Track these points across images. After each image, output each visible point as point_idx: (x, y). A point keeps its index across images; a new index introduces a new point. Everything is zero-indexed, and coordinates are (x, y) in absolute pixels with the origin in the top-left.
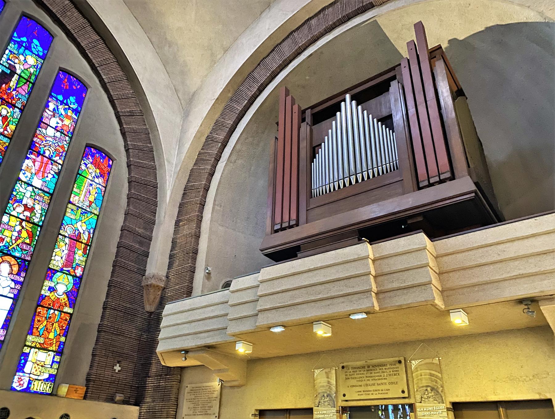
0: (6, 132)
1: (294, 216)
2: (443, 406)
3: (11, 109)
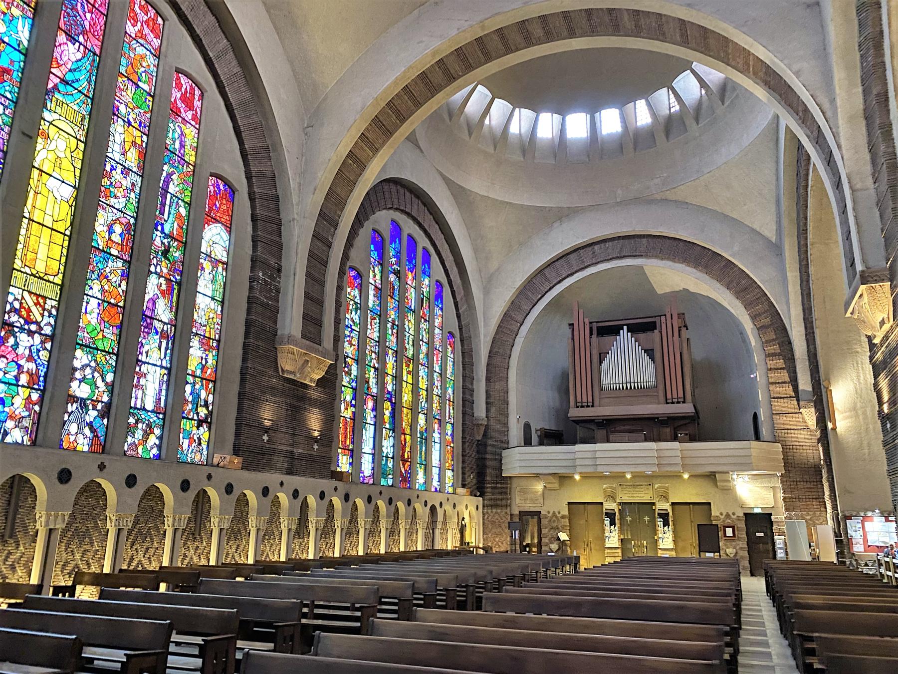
1: (590, 399)
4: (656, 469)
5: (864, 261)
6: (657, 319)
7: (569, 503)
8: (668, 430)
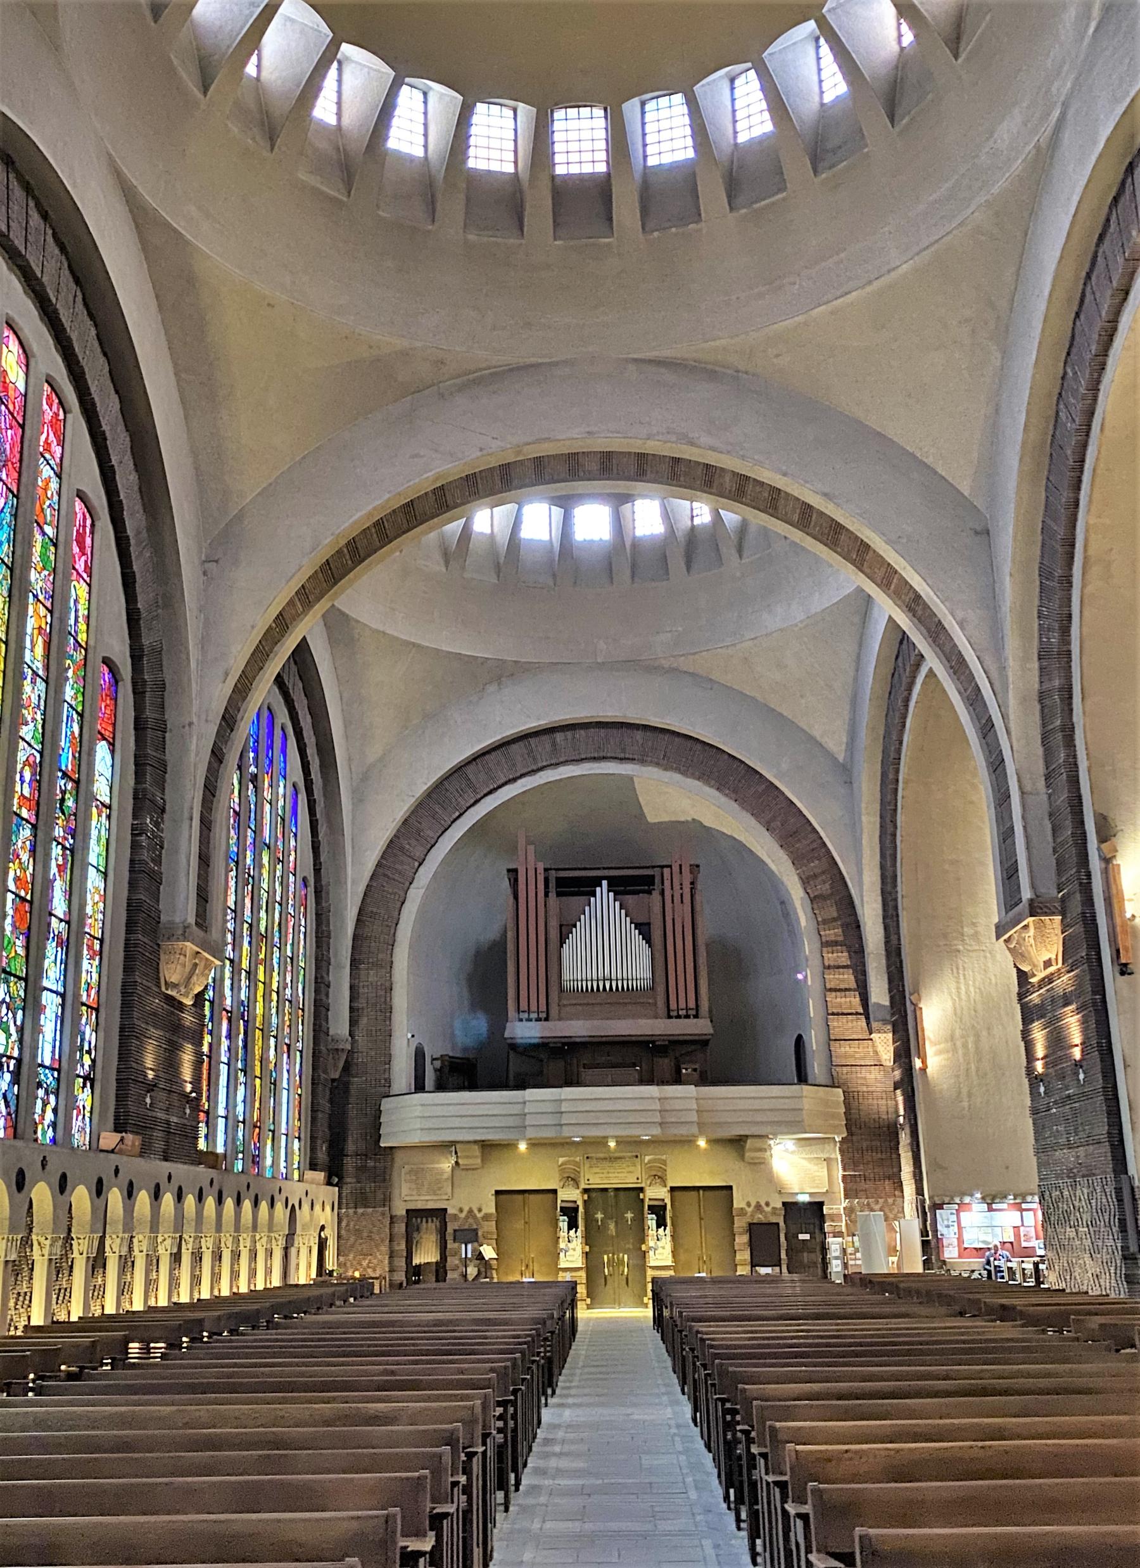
2: (665, 1190)
4: (656, 1131)
5: (1033, 886)
6: (656, 872)
7: (498, 1193)
8: (666, 1061)
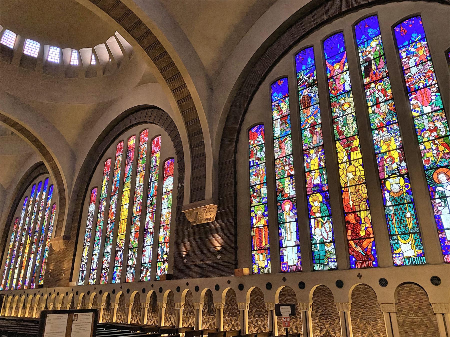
0: (388, 97)
3: (382, 82)
